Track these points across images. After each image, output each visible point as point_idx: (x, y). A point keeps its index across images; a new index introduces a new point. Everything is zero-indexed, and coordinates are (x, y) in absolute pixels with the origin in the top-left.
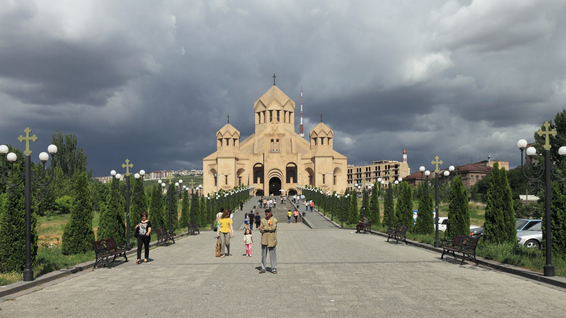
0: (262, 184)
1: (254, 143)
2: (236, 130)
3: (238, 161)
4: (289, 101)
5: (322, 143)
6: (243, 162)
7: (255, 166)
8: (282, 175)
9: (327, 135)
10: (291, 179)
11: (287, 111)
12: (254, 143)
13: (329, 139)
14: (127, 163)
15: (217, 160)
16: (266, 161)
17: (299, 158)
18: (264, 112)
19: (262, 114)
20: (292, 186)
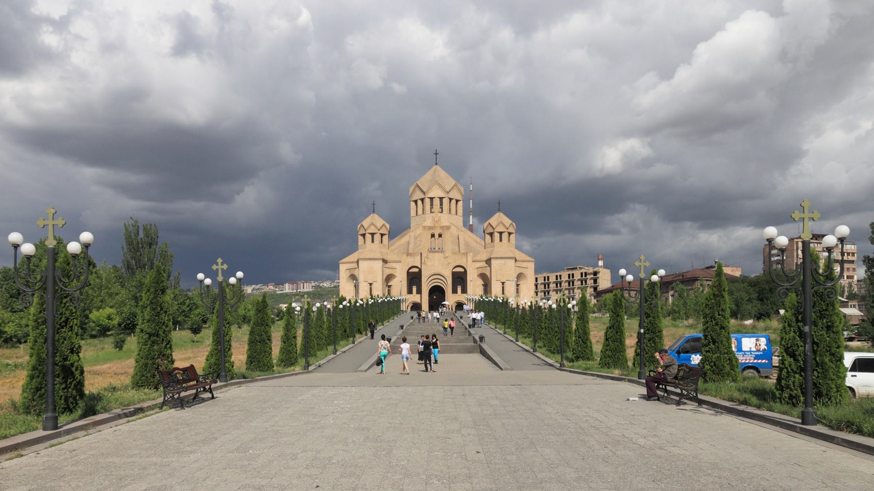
0: (419, 296)
1: (409, 241)
2: (383, 222)
4: (455, 185)
5: (501, 240)
7: (410, 271)
8: (446, 282)
9: (507, 229)
10: (458, 288)
11: (453, 199)
12: (409, 241)
13: (510, 234)
14: (220, 264)
15: (358, 262)
17: (470, 259)
18: (422, 200)
19: (420, 202)
20: (460, 297)
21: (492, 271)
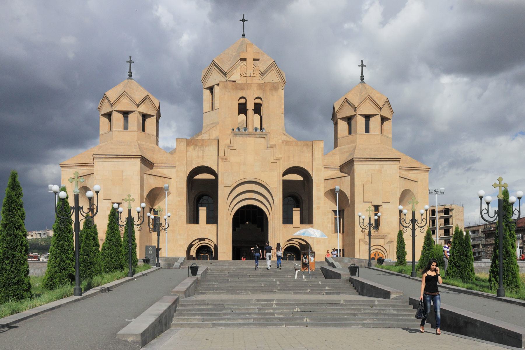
3: (152, 169)
4: (274, 64)
5: (367, 130)
6: (165, 171)
9: (381, 108)
13: (384, 119)
16: (225, 159)
21: (356, 183)
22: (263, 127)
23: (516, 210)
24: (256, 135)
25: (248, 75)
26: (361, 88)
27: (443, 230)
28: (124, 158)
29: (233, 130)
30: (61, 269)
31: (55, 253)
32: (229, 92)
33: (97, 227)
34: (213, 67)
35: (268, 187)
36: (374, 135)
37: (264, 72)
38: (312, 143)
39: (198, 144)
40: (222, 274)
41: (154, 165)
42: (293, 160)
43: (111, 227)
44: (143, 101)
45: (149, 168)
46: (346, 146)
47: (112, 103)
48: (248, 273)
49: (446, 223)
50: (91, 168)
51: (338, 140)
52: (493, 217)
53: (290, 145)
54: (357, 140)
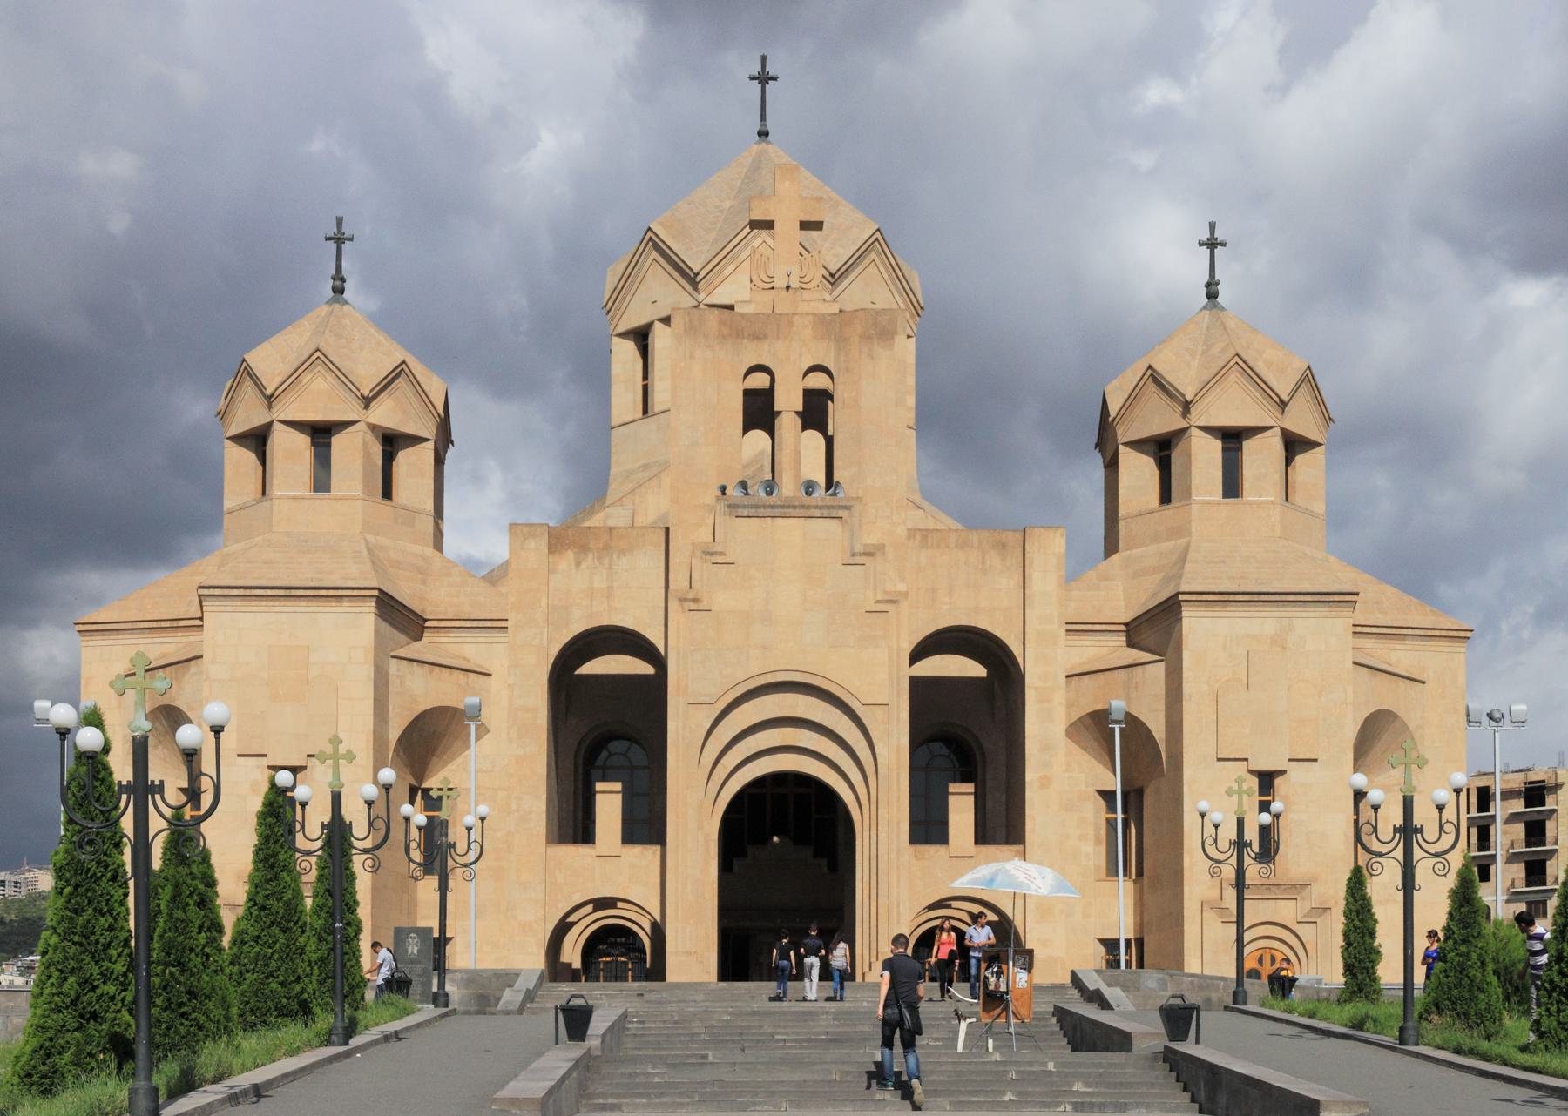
3: (420, 638)
4: (877, 242)
5: (1232, 487)
6: (470, 648)
9: (1283, 405)
13: (1294, 445)
16: (693, 602)
21: (1187, 688)
22: (836, 478)
23: (1448, 822)
24: (808, 507)
25: (780, 282)
26: (1208, 328)
27: (1522, 866)
28: (314, 599)
29: (723, 489)
30: (82, 1016)
31: (59, 956)
32: (709, 346)
33: (214, 860)
34: (648, 256)
35: (855, 706)
36: (1260, 504)
37: (840, 273)
38: (1019, 536)
39: (591, 546)
40: (680, 1035)
41: (428, 624)
42: (950, 603)
43: (265, 860)
44: (385, 385)
45: (407, 634)
46: (1152, 548)
47: (269, 392)
48: (779, 1030)
49: (1533, 839)
50: (192, 639)
51: (1122, 524)
52: (1391, 841)
53: (938, 546)
54: (1194, 525)
